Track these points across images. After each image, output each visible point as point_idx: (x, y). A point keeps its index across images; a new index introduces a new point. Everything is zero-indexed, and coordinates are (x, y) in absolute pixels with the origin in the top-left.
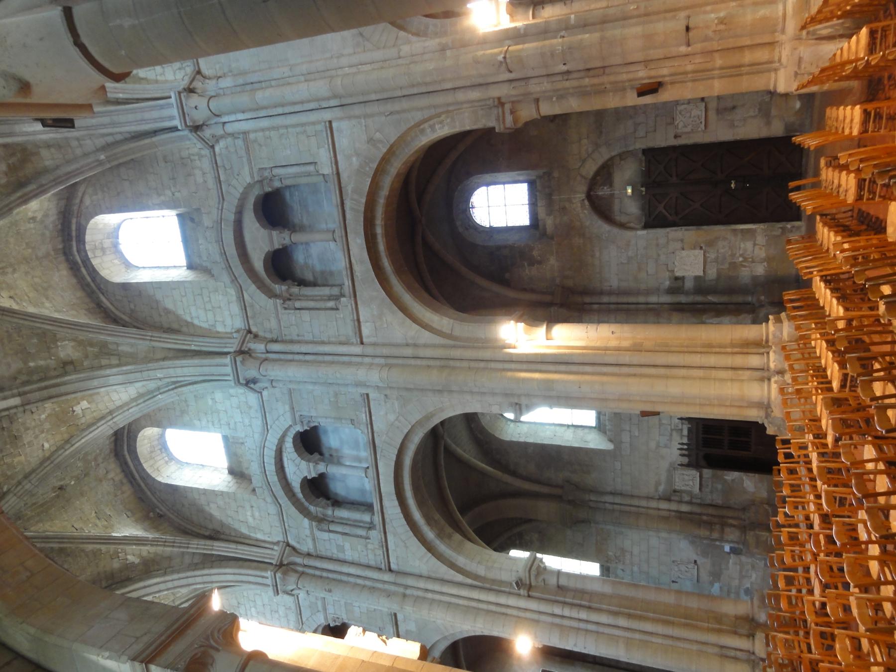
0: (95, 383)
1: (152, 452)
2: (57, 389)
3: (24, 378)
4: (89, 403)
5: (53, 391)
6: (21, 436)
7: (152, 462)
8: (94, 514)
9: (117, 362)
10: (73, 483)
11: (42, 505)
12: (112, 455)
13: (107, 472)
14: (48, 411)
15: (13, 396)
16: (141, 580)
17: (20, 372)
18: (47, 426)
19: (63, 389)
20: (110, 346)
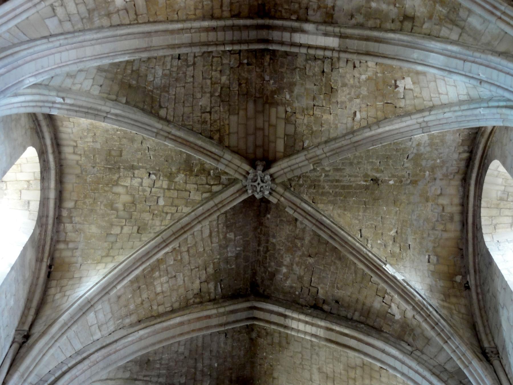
0: (416, 55)
1: (502, 199)
2: (377, 44)
3: (359, 19)
4: (414, 83)
5: (372, 46)
6: (337, 90)
7: (494, 212)
8: (393, 233)
9: (454, 36)
10: (391, 182)
11: (343, 187)
12: (459, 177)
13: (441, 194)
14: (370, 73)
15: (335, 35)
16: (387, 341)
17: (359, 10)
18: (364, 91)
19: (383, 48)
20: (463, 14)
